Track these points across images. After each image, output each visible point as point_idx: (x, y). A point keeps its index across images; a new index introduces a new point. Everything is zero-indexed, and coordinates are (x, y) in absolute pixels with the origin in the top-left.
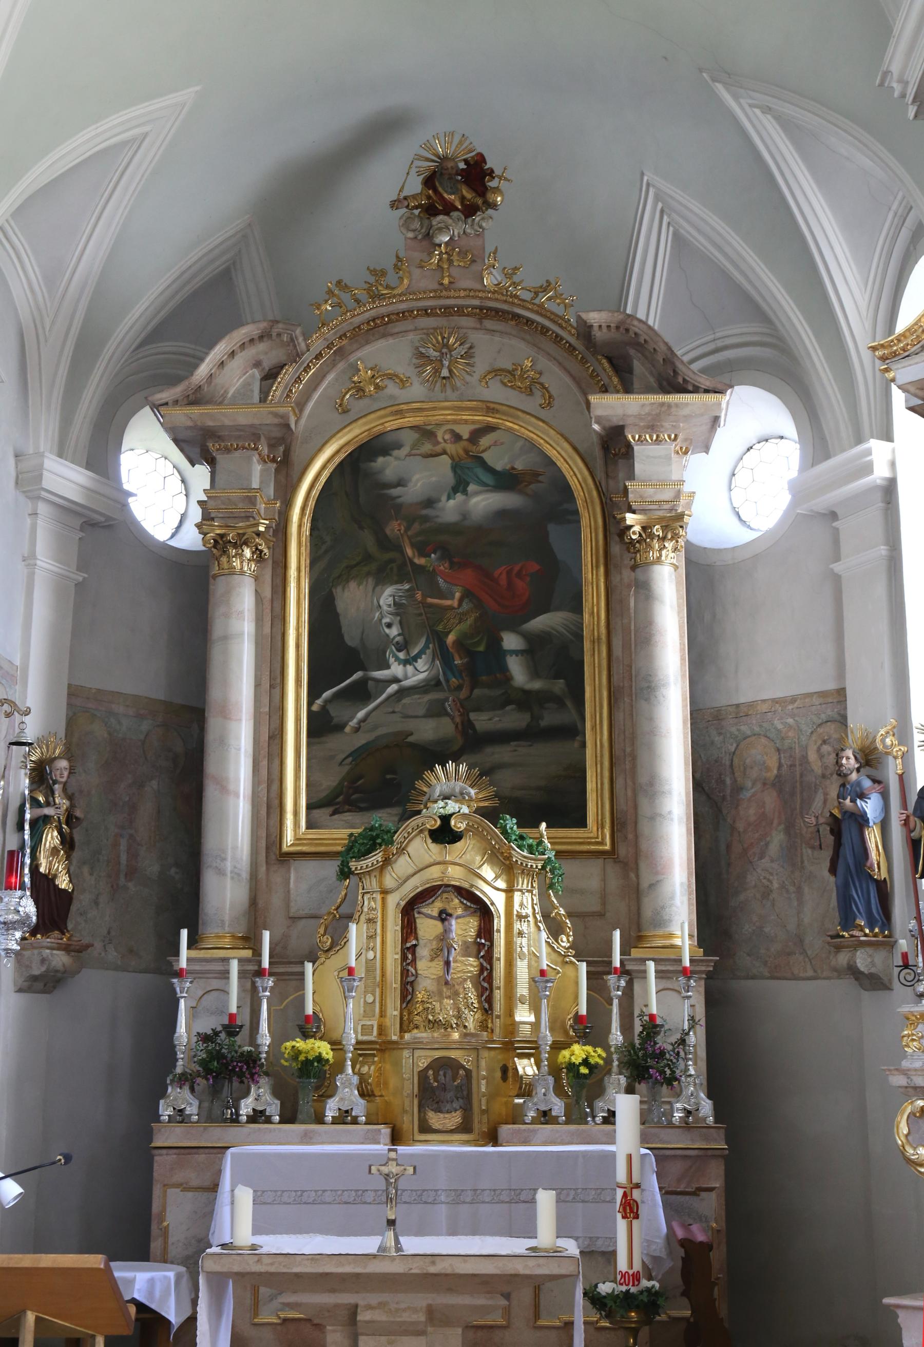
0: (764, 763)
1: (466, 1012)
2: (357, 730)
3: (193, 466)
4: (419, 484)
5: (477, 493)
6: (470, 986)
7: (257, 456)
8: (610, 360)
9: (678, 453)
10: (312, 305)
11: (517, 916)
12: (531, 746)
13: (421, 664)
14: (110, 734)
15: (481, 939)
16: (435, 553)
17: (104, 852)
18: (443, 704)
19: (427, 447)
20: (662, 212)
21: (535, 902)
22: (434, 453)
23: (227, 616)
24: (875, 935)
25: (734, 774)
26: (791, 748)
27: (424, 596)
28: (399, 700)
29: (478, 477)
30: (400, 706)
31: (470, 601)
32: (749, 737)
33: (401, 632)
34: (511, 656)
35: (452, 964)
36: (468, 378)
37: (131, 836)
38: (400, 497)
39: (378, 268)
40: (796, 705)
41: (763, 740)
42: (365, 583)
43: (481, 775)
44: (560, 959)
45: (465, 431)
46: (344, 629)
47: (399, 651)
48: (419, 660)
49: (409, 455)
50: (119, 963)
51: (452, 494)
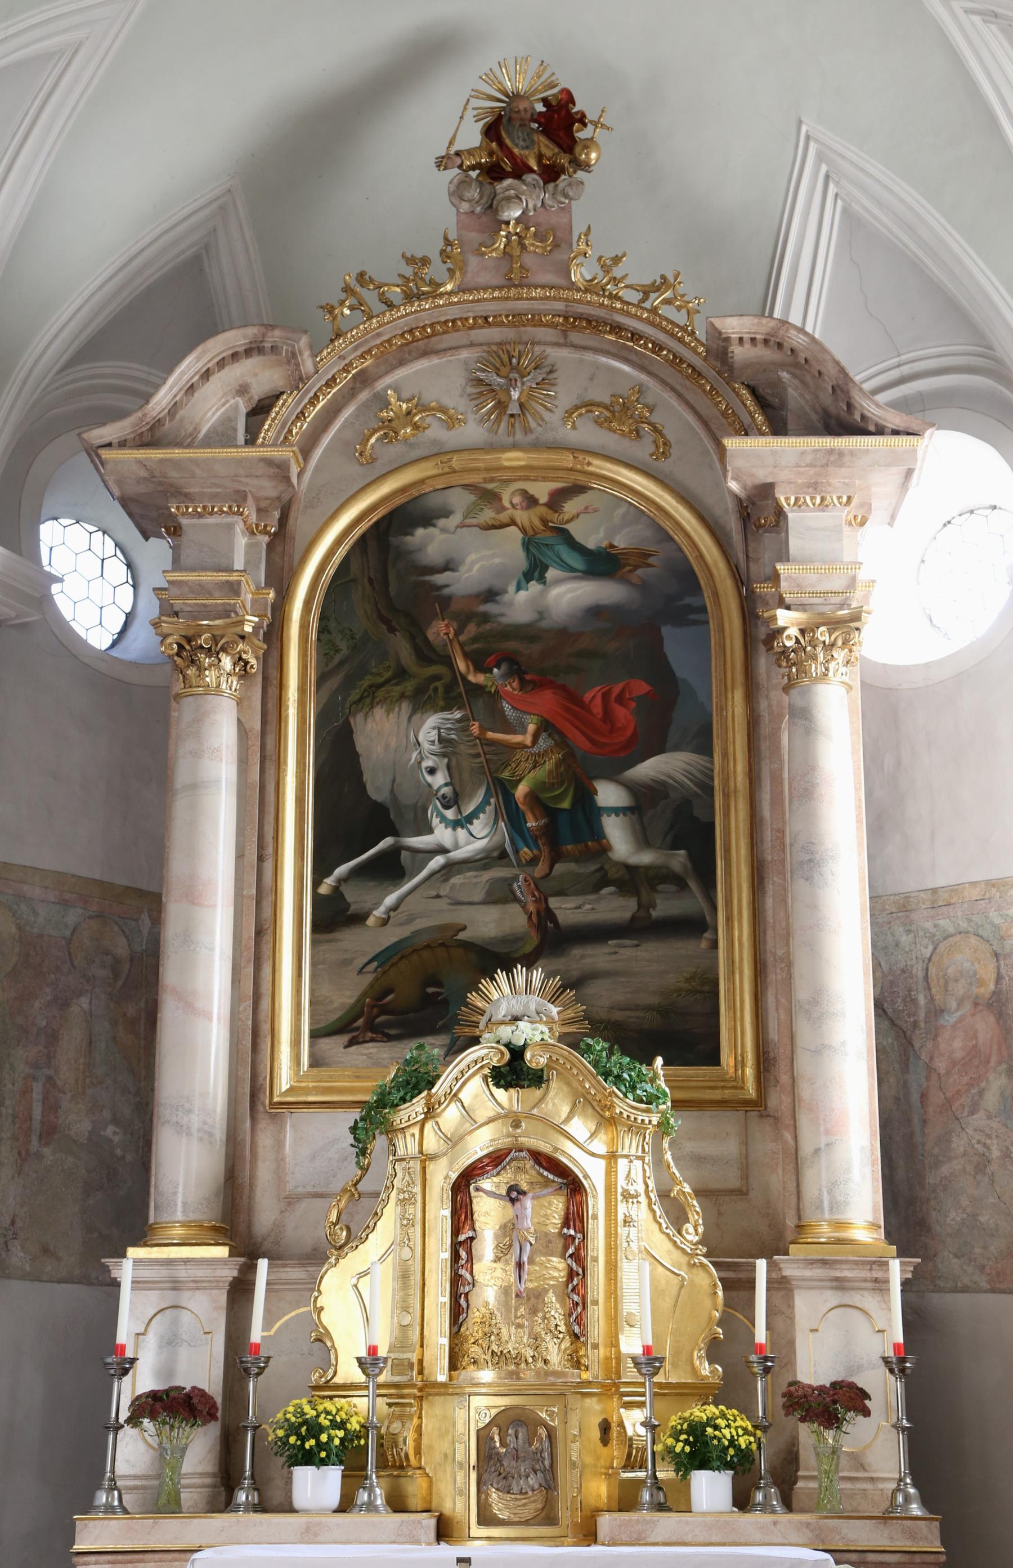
0: (975, 973)
1: (548, 1338)
2: (385, 922)
3: (147, 539)
4: (476, 568)
5: (558, 582)
6: (554, 1299)
7: (241, 524)
8: (753, 391)
9: (850, 524)
10: (322, 307)
11: (622, 1195)
12: (638, 946)
13: (478, 827)
14: (19, 928)
15: (568, 1228)
16: (498, 667)
17: (8, 1102)
18: (511, 885)
19: (488, 515)
20: (827, 177)
21: (648, 1174)
22: (496, 524)
23: (197, 754)
25: (930, 989)
27: (483, 729)
28: (446, 880)
29: (562, 560)
30: (448, 889)
31: (550, 735)
32: (952, 936)
33: (449, 780)
34: (609, 816)
35: (526, 1266)
36: (546, 415)
37: (50, 1079)
38: (447, 586)
39: (419, 255)
41: (973, 940)
42: (397, 709)
43: (564, 987)
44: (684, 1260)
45: (542, 491)
46: (367, 777)
47: (447, 807)
48: (475, 821)
49: (461, 526)
50: (28, 1268)
51: (523, 582)
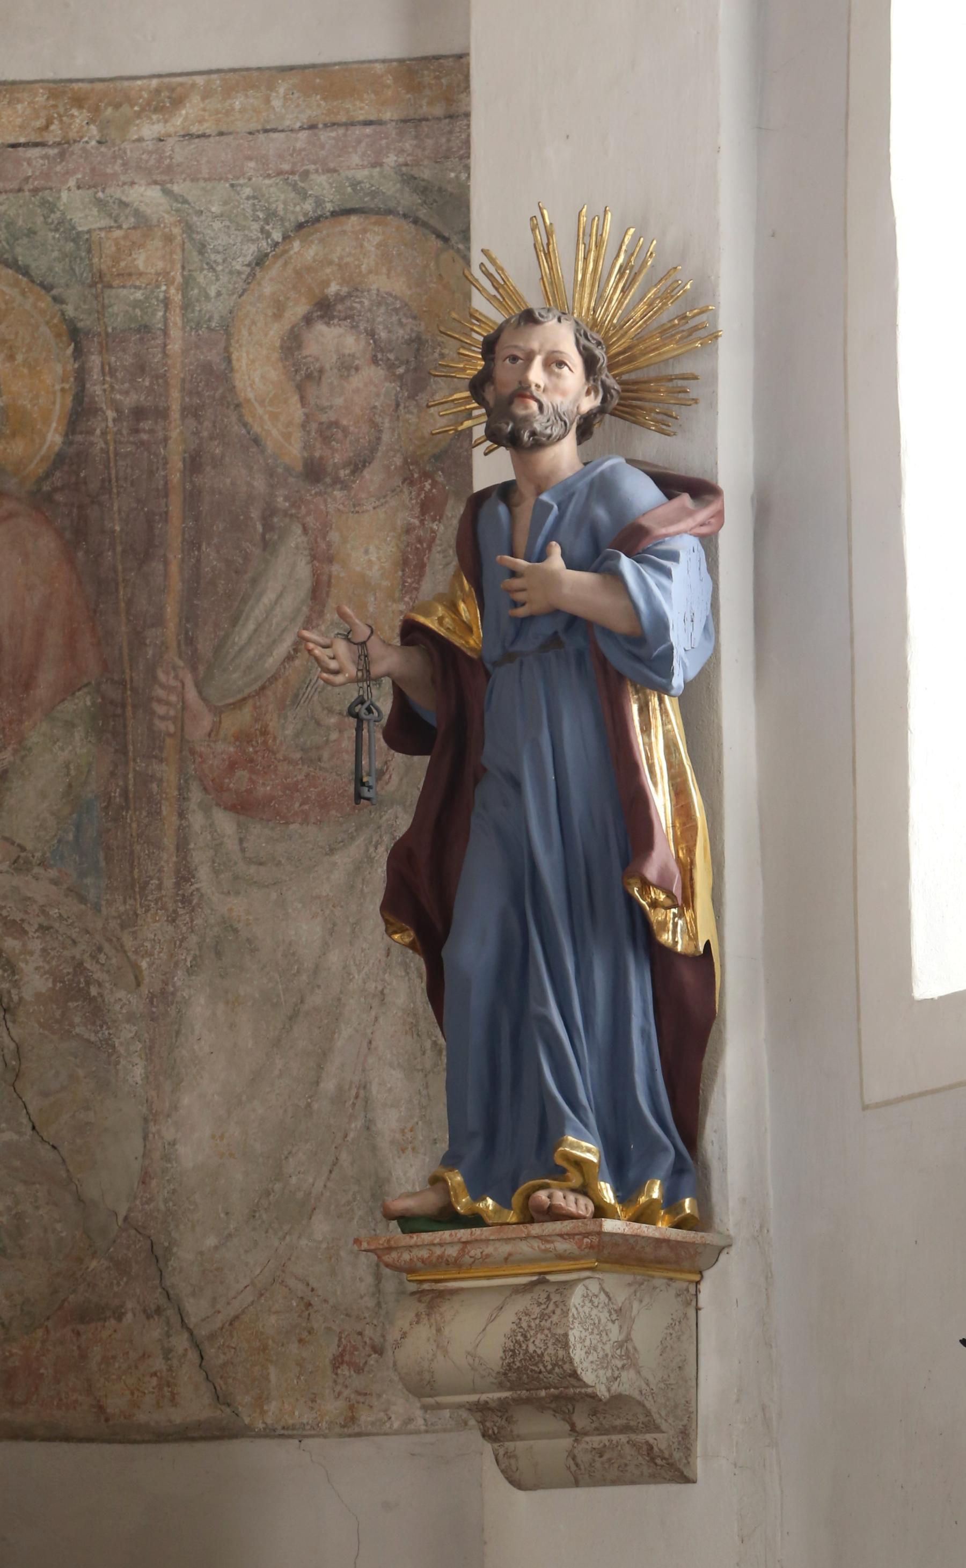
24: (644, 1216)
26: (145, 329)
40: (177, 122)
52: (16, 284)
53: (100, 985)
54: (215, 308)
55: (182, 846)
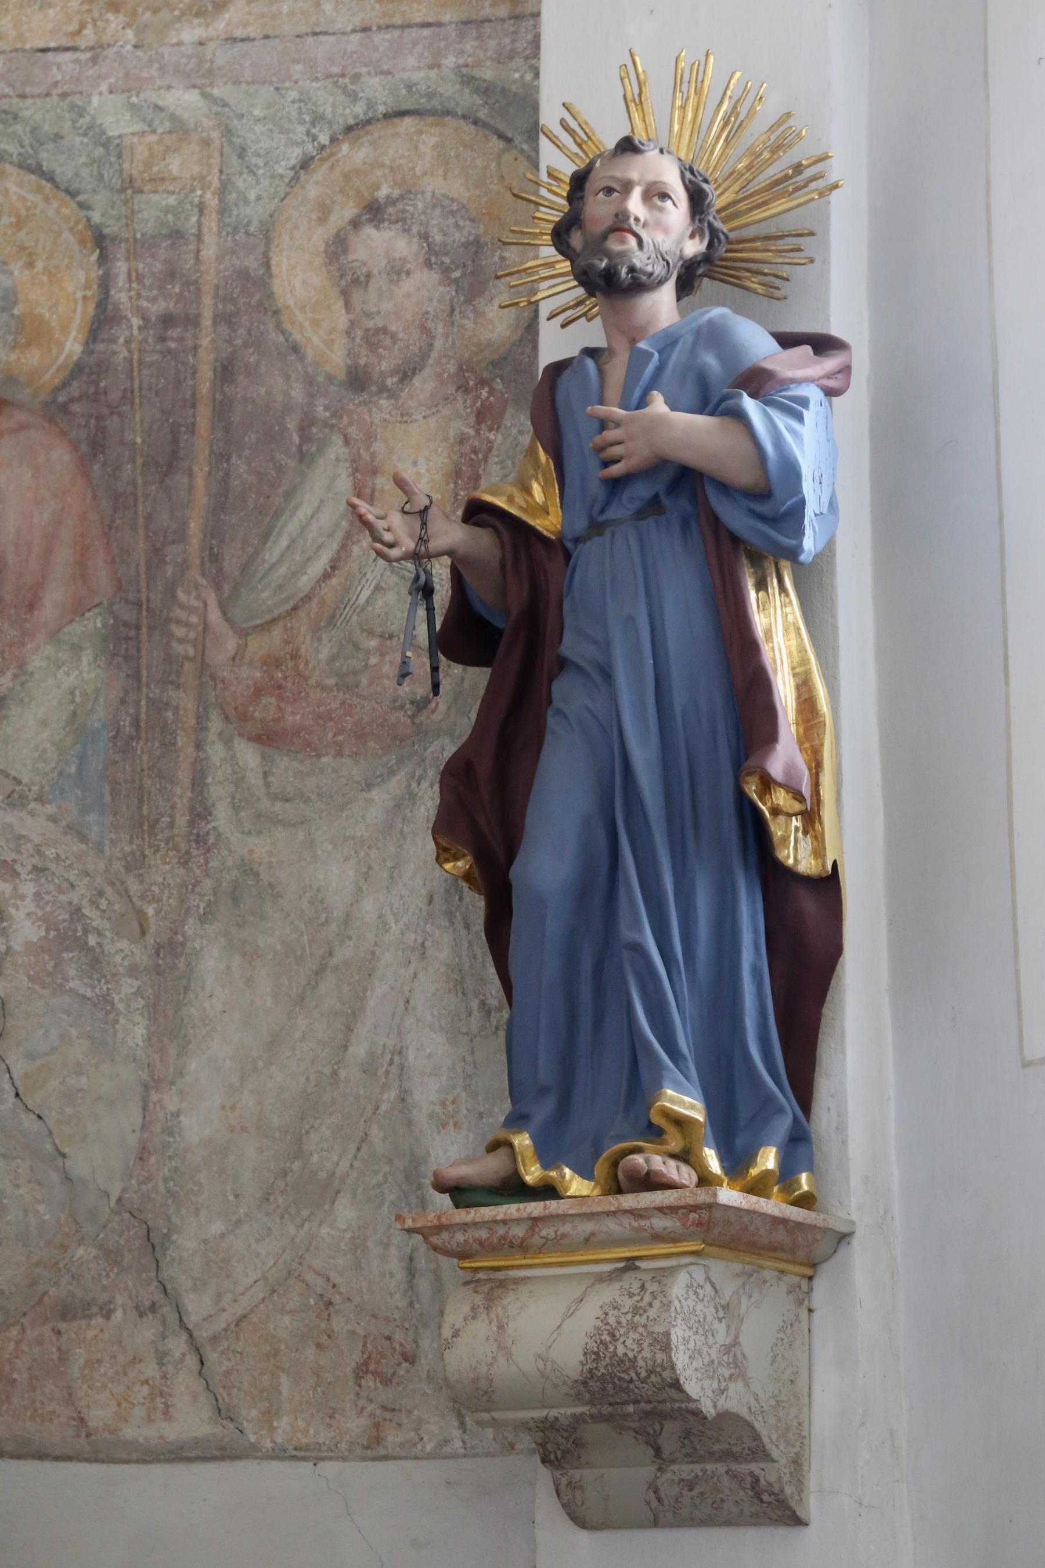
24: (758, 1188)
26: (176, 235)
40: (220, 25)
52: (39, 190)
53: (100, 934)
54: (254, 213)
55: (199, 780)
